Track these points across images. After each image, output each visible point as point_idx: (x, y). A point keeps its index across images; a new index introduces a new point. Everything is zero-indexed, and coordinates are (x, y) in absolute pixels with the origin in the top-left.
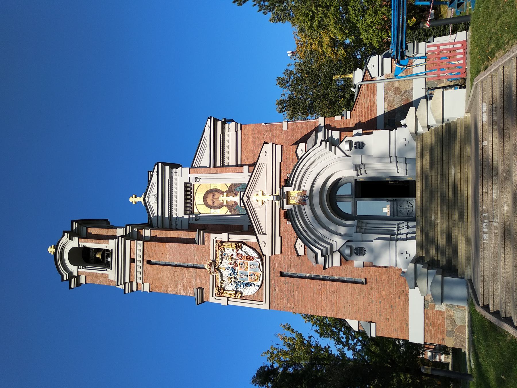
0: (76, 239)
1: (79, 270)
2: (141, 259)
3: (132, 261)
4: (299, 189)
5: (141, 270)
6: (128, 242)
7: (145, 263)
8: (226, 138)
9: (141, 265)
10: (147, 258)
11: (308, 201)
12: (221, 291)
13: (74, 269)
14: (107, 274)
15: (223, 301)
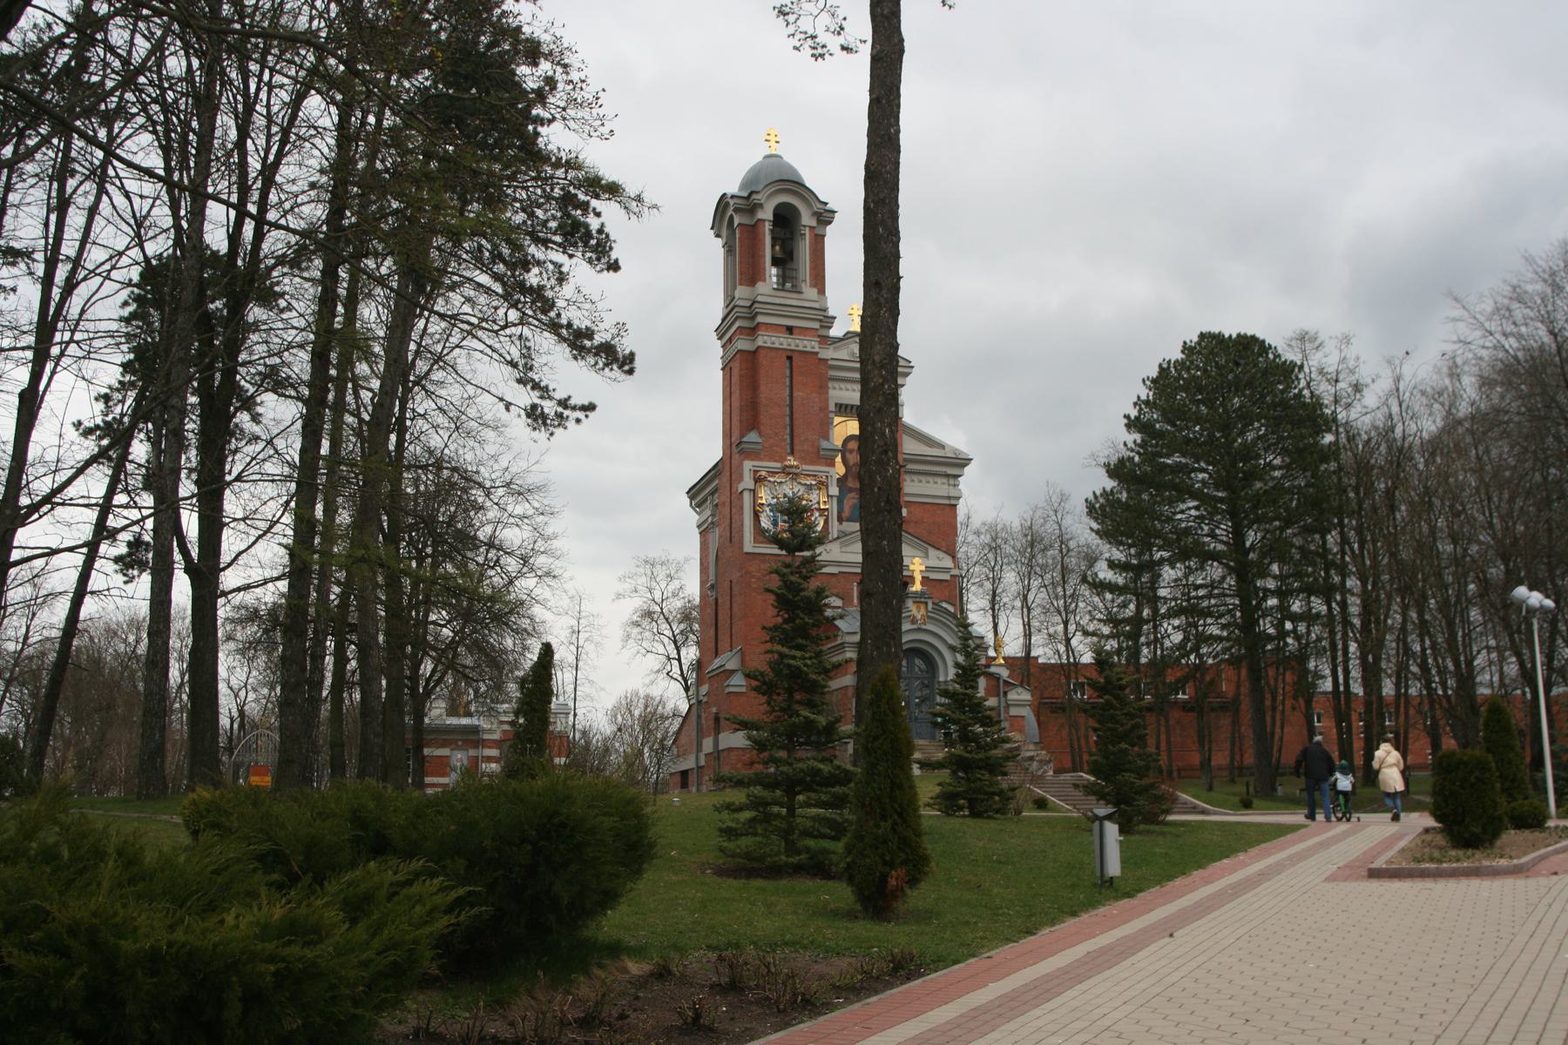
0: (814, 223)
1: (767, 223)
2: (793, 347)
3: (790, 330)
4: (929, 617)
5: (777, 345)
6: (816, 325)
7: (789, 354)
8: (939, 480)
9: (785, 346)
10: (795, 356)
11: (915, 627)
12: (758, 480)
13: (767, 214)
14: (764, 280)
15: (748, 482)
